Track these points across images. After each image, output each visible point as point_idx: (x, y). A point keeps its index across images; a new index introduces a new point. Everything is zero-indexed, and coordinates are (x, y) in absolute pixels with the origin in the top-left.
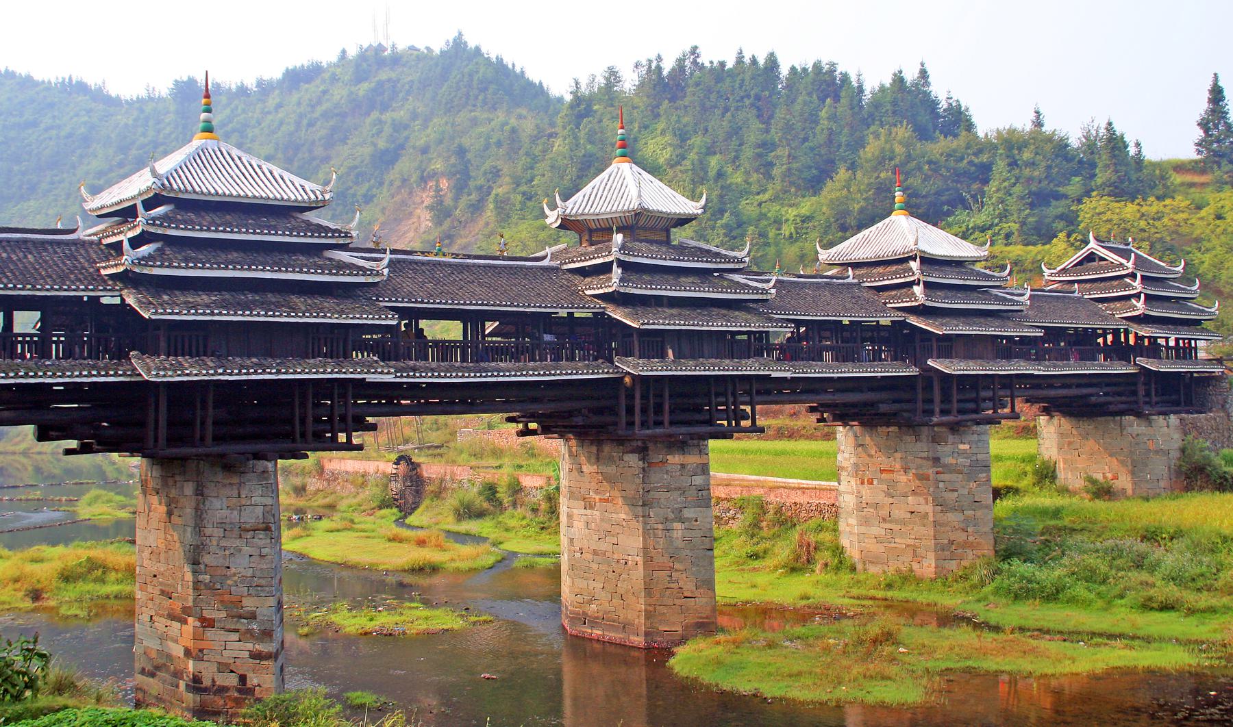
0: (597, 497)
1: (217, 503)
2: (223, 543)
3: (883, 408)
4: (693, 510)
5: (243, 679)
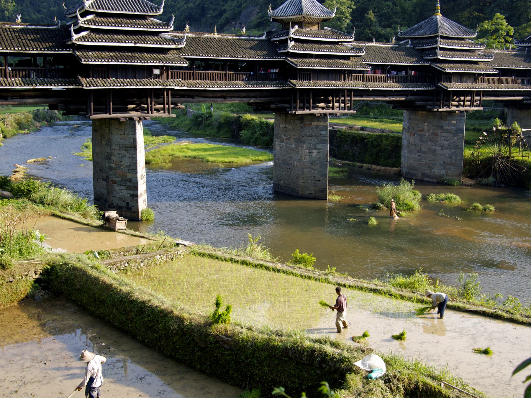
1: (116, 136)
2: (119, 152)
3: (417, 103)
4: (321, 145)
5: (128, 203)
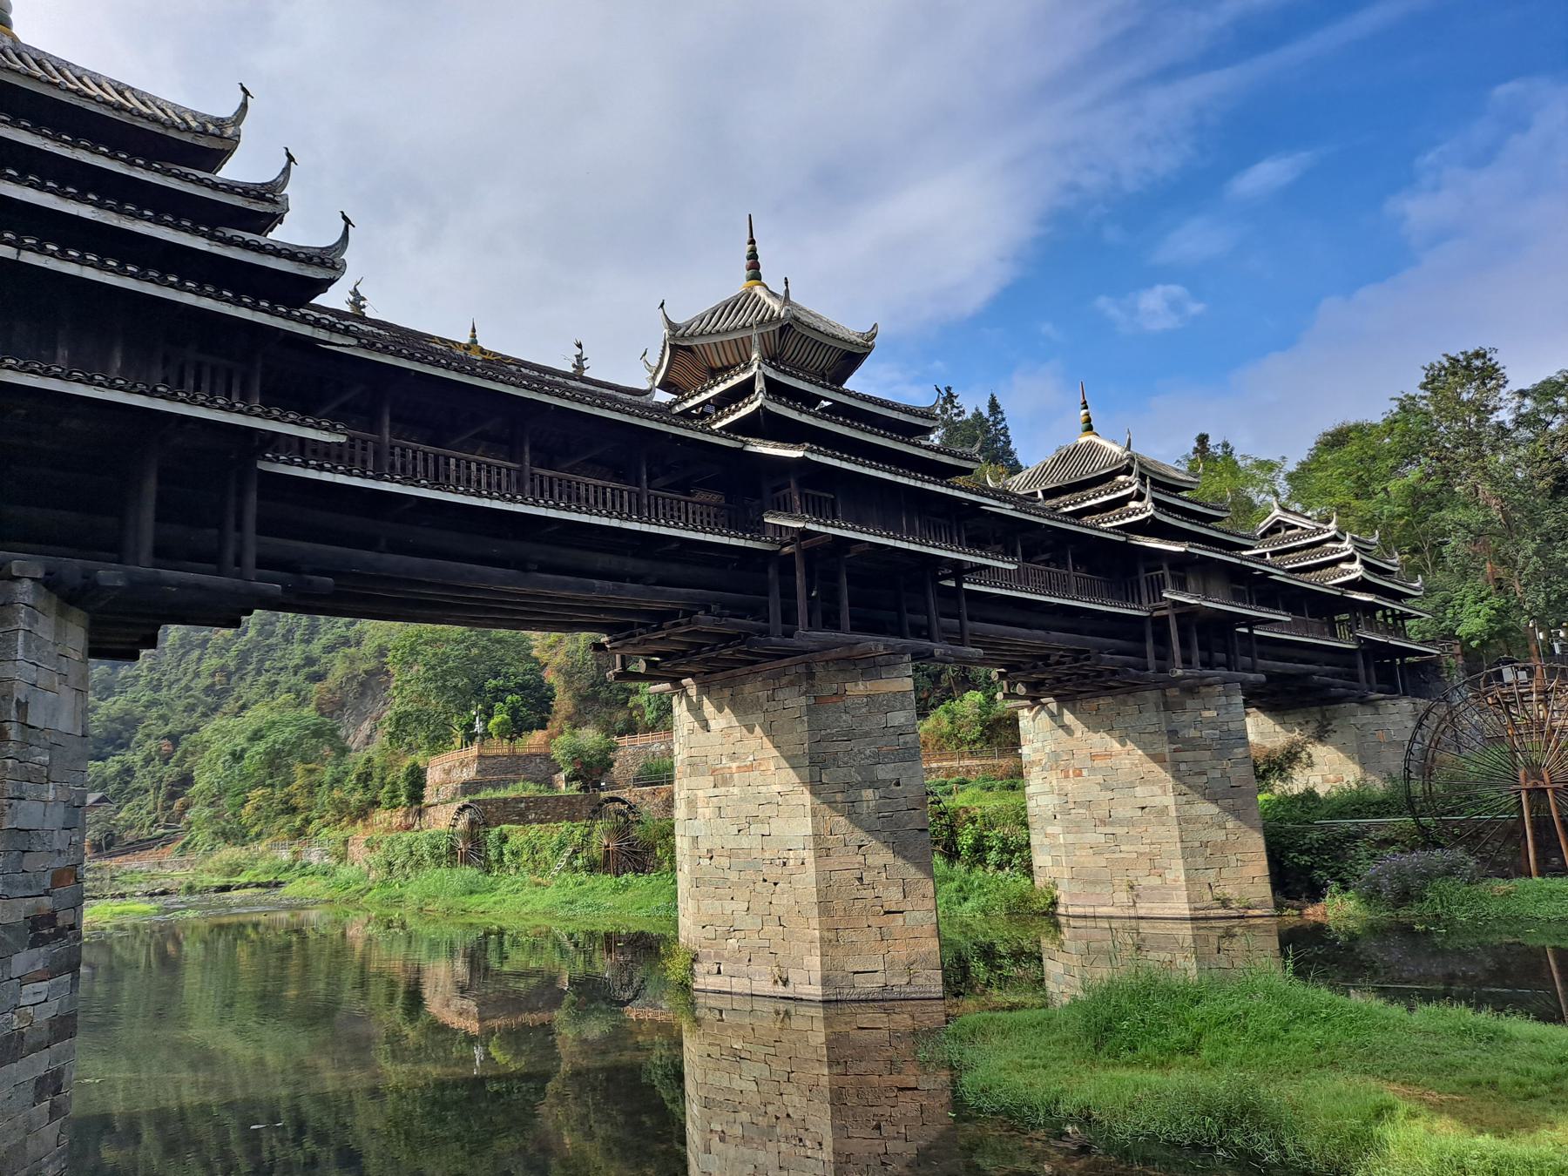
0: (734, 765)
